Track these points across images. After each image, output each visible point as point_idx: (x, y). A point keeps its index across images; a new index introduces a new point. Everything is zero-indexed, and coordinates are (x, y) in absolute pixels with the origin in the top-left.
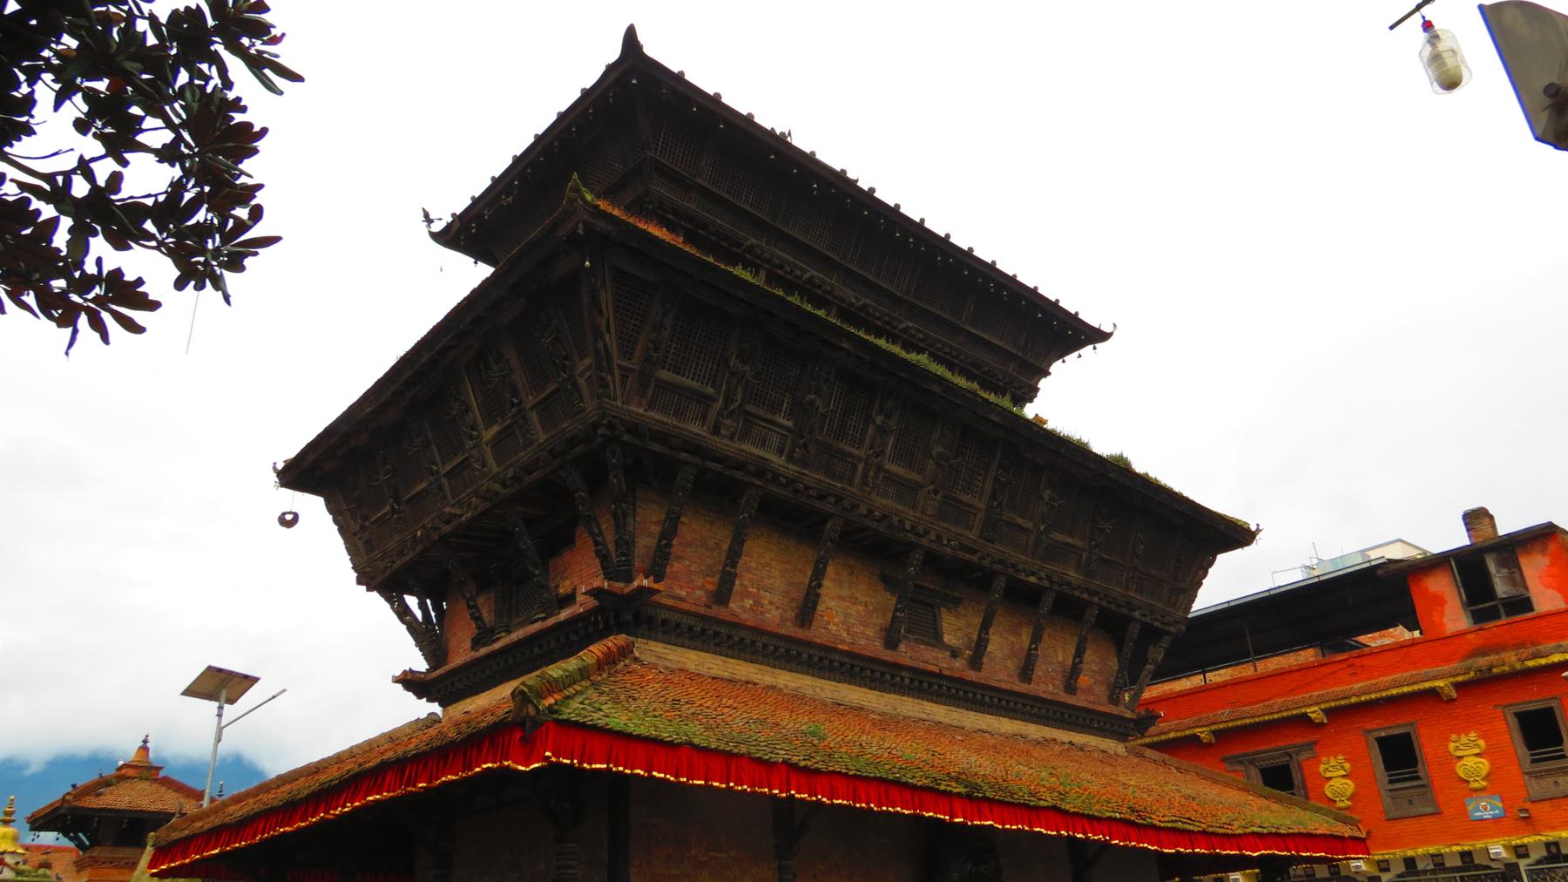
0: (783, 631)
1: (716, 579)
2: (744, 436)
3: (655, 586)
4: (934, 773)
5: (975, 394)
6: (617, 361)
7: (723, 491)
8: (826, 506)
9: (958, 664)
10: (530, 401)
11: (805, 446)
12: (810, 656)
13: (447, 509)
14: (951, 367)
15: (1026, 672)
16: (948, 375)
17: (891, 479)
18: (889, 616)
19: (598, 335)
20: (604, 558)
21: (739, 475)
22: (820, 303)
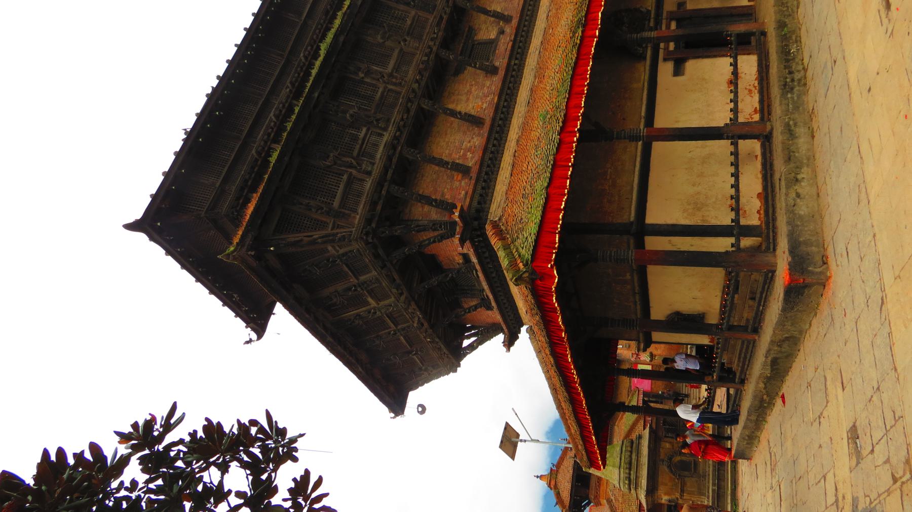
0: (486, 135)
1: (455, 174)
2: (372, 156)
3: (459, 208)
4: (570, 47)
5: (345, 14)
6: (329, 231)
7: (404, 170)
8: (413, 108)
9: (508, 30)
10: (353, 280)
11: (377, 120)
12: (501, 119)
13: (415, 325)
14: (328, 29)
16: (333, 31)
17: (397, 68)
18: (478, 71)
19: (314, 242)
20: (442, 238)
21: (394, 160)
22: (291, 110)
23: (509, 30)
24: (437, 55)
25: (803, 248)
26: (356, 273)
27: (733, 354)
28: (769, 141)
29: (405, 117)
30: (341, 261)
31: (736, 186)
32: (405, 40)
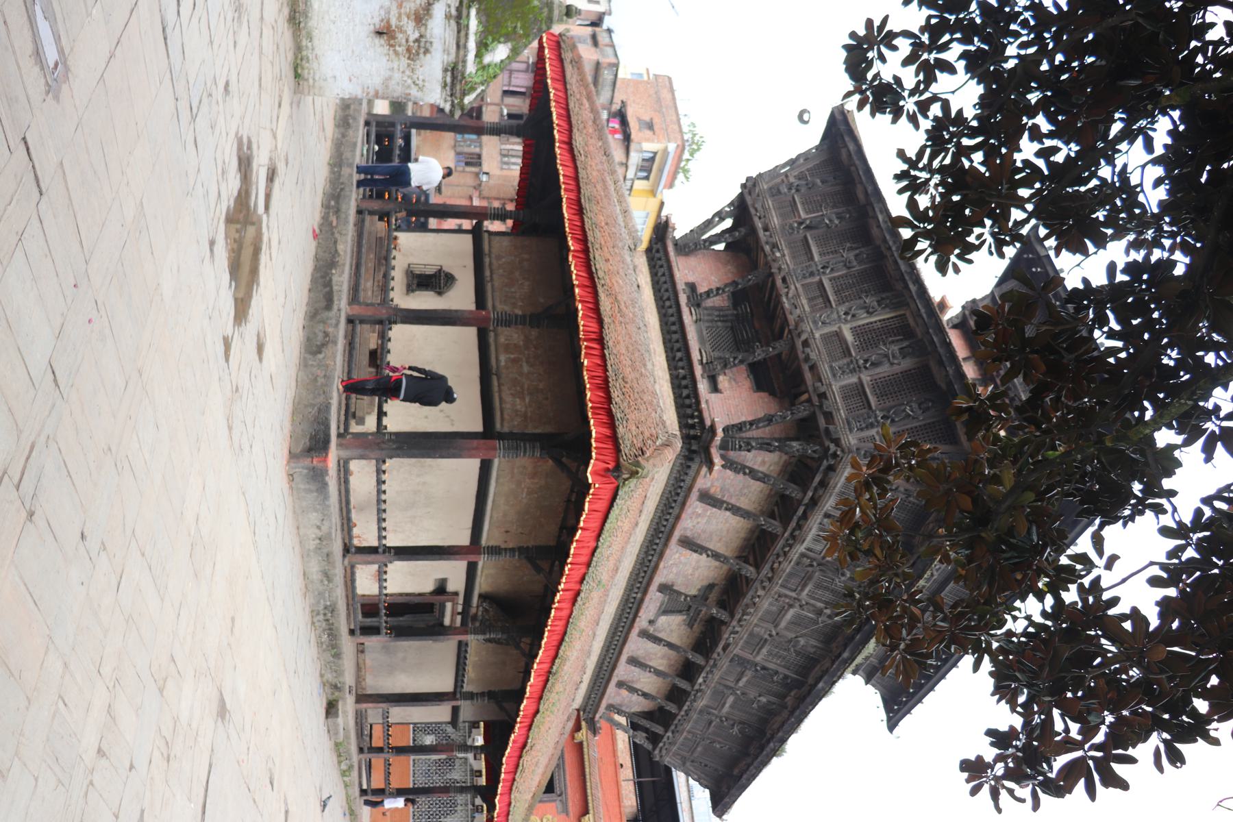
7: (784, 507)
11: (811, 566)
15: (633, 661)
17: (782, 611)
20: (740, 427)
21: (793, 524)
23: (642, 622)
24: (732, 616)
25: (313, 487)
26: (859, 389)
27: (370, 233)
28: (345, 545)
29: (776, 565)
30: (876, 417)
31: (380, 482)
32: (770, 635)
